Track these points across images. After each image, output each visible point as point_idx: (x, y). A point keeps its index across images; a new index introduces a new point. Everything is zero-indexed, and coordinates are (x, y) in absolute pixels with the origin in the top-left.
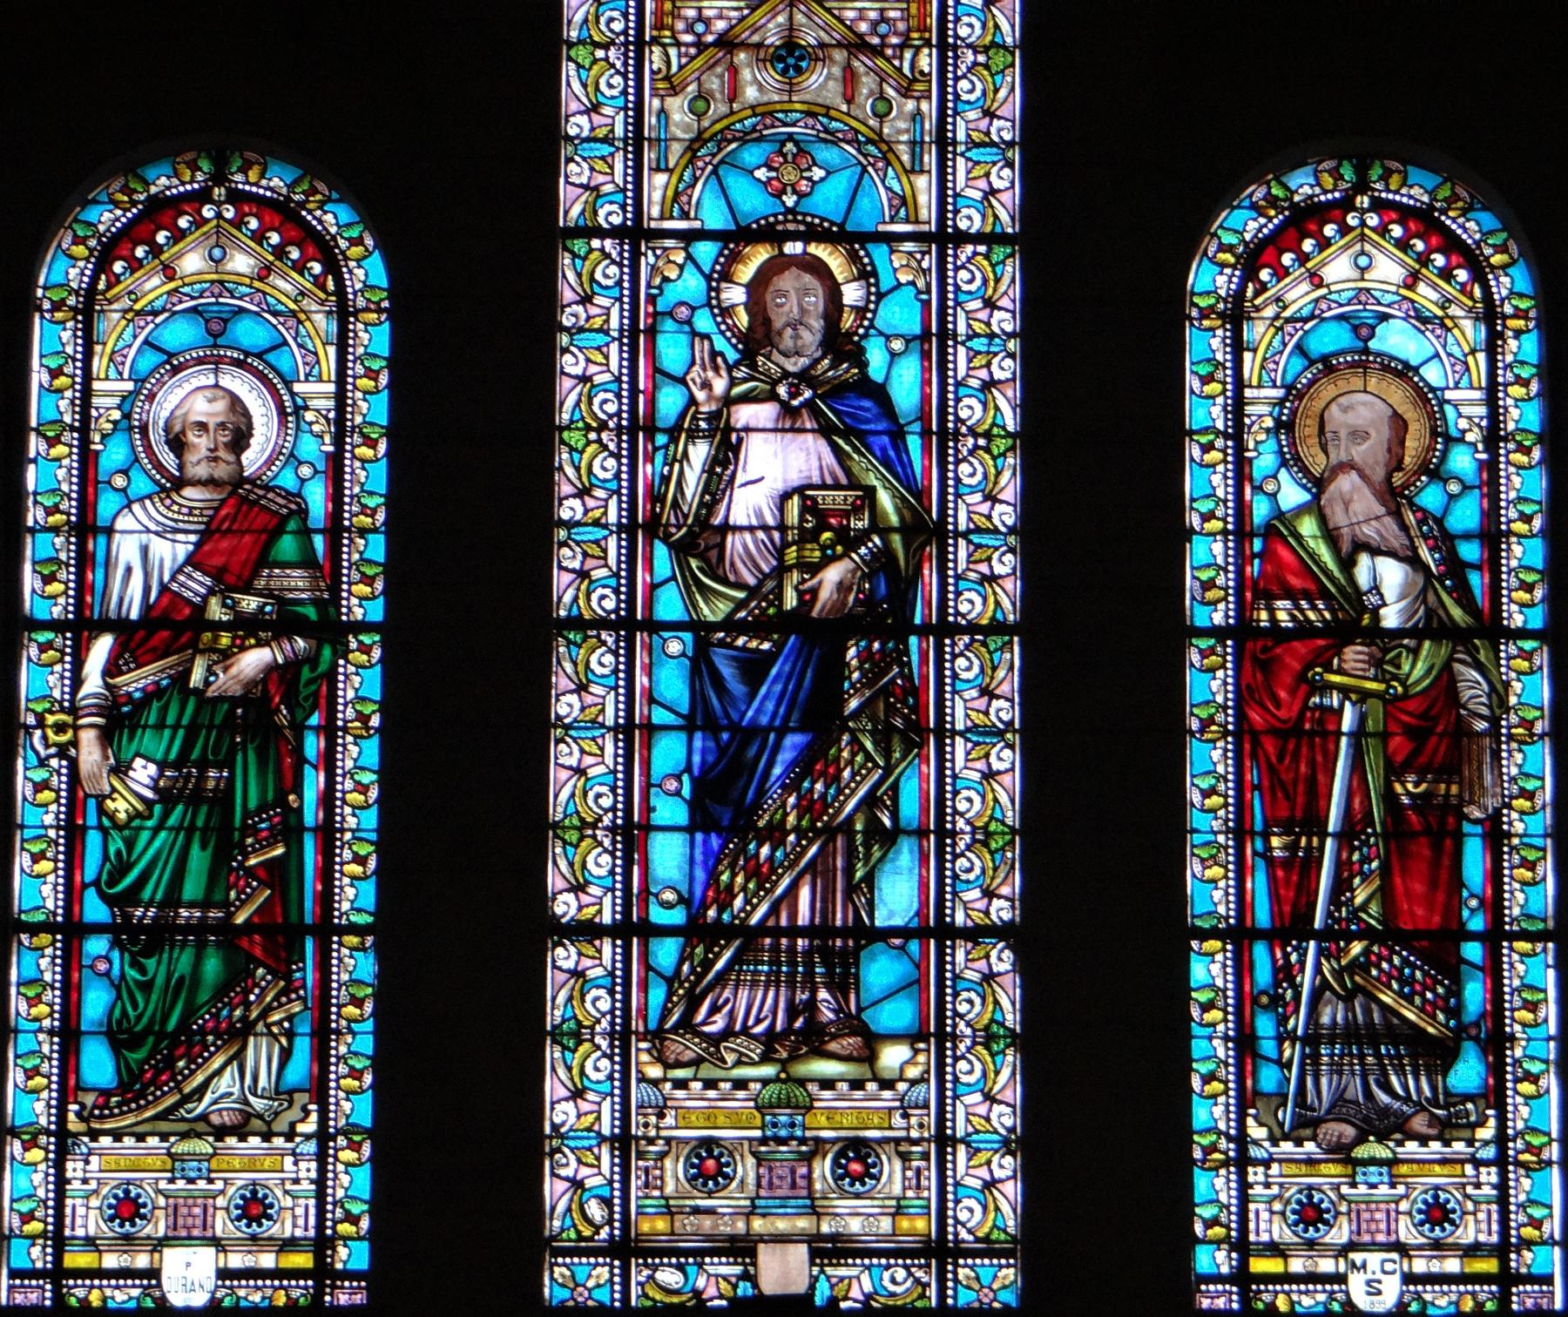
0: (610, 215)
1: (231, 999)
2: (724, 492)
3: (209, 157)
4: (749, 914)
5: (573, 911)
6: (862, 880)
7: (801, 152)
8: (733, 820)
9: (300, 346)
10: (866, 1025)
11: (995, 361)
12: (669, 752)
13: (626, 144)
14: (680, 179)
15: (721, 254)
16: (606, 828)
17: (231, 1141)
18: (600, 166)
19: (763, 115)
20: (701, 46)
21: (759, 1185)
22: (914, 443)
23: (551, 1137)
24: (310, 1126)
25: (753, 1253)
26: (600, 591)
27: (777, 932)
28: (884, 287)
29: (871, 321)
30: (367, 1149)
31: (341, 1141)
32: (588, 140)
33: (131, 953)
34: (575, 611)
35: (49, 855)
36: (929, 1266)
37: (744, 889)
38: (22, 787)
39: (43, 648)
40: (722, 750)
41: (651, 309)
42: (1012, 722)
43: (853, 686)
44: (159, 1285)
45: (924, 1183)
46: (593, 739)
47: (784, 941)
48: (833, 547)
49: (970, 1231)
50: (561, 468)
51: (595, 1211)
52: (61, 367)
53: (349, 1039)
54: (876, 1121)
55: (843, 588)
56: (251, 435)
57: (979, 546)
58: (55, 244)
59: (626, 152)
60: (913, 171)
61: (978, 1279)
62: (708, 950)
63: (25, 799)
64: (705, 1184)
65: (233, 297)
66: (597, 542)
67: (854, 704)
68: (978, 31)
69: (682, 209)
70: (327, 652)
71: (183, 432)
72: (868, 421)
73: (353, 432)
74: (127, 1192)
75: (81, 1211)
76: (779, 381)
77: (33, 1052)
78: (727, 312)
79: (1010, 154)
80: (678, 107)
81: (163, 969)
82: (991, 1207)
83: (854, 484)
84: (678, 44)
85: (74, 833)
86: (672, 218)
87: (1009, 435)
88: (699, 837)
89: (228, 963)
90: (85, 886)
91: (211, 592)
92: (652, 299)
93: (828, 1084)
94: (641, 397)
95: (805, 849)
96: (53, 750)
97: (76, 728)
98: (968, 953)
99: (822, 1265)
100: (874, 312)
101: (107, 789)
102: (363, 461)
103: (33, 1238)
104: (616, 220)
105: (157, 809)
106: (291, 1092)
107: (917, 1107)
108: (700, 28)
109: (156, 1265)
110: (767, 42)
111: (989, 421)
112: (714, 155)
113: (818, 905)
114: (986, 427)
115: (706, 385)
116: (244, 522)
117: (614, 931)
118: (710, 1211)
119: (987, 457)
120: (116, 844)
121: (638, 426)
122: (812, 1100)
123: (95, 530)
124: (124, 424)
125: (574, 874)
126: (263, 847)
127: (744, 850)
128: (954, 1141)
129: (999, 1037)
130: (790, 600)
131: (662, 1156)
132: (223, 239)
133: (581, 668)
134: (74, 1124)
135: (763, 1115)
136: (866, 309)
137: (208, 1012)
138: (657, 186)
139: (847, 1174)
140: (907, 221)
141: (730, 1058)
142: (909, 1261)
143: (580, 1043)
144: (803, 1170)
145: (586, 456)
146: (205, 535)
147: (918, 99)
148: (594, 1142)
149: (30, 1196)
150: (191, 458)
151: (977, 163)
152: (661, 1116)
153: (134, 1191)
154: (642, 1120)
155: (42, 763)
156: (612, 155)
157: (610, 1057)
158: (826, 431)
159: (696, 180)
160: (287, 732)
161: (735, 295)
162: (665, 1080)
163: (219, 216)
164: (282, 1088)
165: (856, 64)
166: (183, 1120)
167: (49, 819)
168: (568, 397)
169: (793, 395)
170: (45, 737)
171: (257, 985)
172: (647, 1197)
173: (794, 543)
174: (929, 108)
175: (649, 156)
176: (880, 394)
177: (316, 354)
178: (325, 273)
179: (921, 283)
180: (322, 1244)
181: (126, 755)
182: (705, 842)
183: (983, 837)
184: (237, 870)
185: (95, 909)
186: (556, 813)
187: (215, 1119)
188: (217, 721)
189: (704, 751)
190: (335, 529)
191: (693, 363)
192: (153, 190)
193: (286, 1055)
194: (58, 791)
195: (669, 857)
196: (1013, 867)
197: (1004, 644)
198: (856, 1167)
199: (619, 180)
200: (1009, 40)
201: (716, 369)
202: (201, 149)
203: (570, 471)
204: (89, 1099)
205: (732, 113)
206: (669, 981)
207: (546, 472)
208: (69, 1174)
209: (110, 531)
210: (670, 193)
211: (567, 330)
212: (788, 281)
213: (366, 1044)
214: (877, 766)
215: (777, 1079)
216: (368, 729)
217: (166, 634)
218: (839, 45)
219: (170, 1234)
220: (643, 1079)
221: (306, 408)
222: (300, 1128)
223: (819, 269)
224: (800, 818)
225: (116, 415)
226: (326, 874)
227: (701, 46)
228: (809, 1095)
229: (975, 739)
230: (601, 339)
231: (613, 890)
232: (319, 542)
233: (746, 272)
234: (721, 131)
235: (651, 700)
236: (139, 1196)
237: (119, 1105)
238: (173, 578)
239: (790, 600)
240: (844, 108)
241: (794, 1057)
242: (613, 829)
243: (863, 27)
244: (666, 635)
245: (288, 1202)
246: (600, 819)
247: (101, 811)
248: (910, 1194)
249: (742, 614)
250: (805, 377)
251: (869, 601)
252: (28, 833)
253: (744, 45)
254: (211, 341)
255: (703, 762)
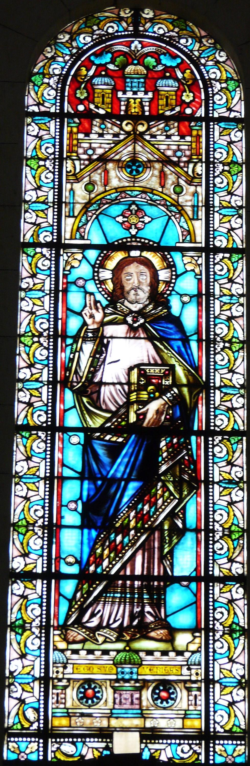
0: (45, 237)
2: (100, 366)
4: (111, 569)
5: (22, 566)
6: (168, 553)
7: (139, 209)
8: (103, 523)
10: (169, 624)
11: (234, 308)
12: (71, 490)
13: (54, 205)
14: (80, 221)
15: (99, 256)
16: (40, 526)
18: (41, 214)
19: (121, 192)
20: (91, 161)
21: (114, 703)
22: (194, 345)
23: (9, 678)
25: (111, 737)
26: (38, 413)
27: (125, 578)
28: (179, 273)
29: (173, 287)
32: (35, 202)
34: (25, 422)
36: (200, 744)
37: (109, 557)
40: (98, 489)
41: (65, 281)
42: (241, 479)
43: (163, 459)
45: (198, 702)
46: (34, 483)
47: (128, 582)
48: (154, 393)
49: (222, 727)
50: (20, 354)
51: (31, 714)
54: (175, 671)
55: (158, 412)
57: (226, 394)
59: (54, 208)
60: (193, 219)
61: (225, 751)
62: (90, 586)
64: (87, 702)
66: (37, 389)
67: (164, 468)
68: (225, 155)
69: (81, 235)
72: (171, 334)
76: (128, 315)
78: (102, 282)
79: (240, 212)
80: (79, 188)
82: (233, 715)
83: (164, 363)
84: (80, 159)
86: (76, 239)
87: (241, 342)
88: (86, 531)
92: (65, 276)
93: (150, 653)
94: (60, 322)
95: (139, 538)
98: (221, 589)
99: (146, 743)
100: (174, 283)
104: (49, 239)
107: (195, 665)
108: (90, 152)
110: (123, 159)
111: (231, 335)
112: (97, 210)
113: (146, 565)
114: (230, 338)
115: (92, 316)
117: (42, 576)
118: (90, 715)
119: (230, 352)
121: (58, 335)
122: (142, 661)
125: (23, 548)
127: (108, 538)
128: (214, 682)
129: (237, 631)
130: (133, 418)
131: (65, 687)
133: (28, 449)
135: (117, 668)
136: (170, 282)
138: (68, 224)
139: (159, 697)
140: (191, 242)
141: (101, 639)
142: (190, 742)
143: (24, 630)
144: (137, 695)
145: (32, 349)
147: (196, 186)
148: (31, 680)
151: (225, 216)
152: (65, 667)
154: (55, 669)
156: (47, 209)
157: (40, 638)
158: (150, 338)
159: (88, 221)
161: (106, 275)
162: (67, 649)
165: (166, 169)
168: (23, 319)
169: (134, 322)
172: (57, 708)
173: (135, 391)
174: (201, 190)
175: (65, 210)
176: (177, 322)
179: (197, 271)
182: (89, 534)
183: (228, 533)
186: (14, 519)
189: (89, 490)
191: (85, 306)
195: (72, 542)
196: (243, 548)
197: (239, 441)
198: (164, 694)
199: (50, 220)
200: (240, 160)
201: (97, 309)
203: (24, 356)
205: (106, 191)
206: (70, 601)
207: (13, 355)
210: (75, 228)
211: (24, 290)
212: (133, 268)
214: (175, 498)
215: (124, 650)
218: (158, 161)
220: (56, 649)
223: (148, 263)
224: (137, 523)
227: (91, 161)
228: (141, 658)
229: (224, 485)
230: (40, 294)
231: (42, 556)
233: (111, 264)
234: (100, 199)
235: (63, 465)
239: (133, 418)
240: (160, 190)
241: (133, 639)
242: (43, 527)
243: (169, 153)
244: (70, 434)
246: (36, 522)
248: (191, 708)
249: (109, 424)
250: (141, 313)
251: (172, 419)
253: (112, 160)
255: (88, 495)
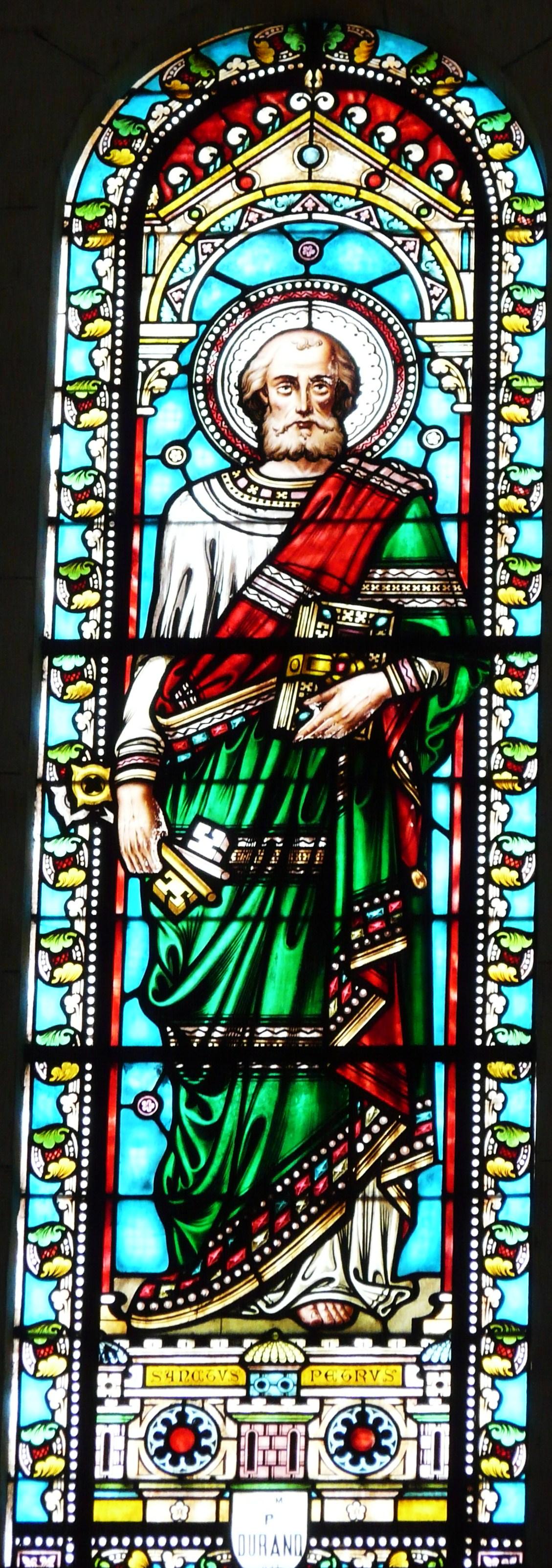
1: (331, 1151)
3: (299, 31)
9: (424, 275)
17: (330, 1345)
24: (443, 1323)
30: (522, 1354)
31: (487, 1344)
33: (189, 1088)
35: (77, 954)
38: (39, 865)
39: (69, 677)
44: (227, 1545)
52: (95, 307)
53: (497, 1203)
56: (356, 393)
58: (88, 147)
63: (42, 879)
65: (332, 212)
70: (463, 679)
71: (264, 389)
73: (498, 386)
74: (182, 1416)
75: (117, 1443)
77: (52, 1224)
81: (234, 1108)
85: (109, 927)
89: (324, 1099)
90: (125, 997)
91: (303, 600)
96: (82, 814)
97: (115, 785)
101: (157, 867)
102: (512, 424)
103: (50, 1480)
105: (227, 892)
106: (415, 1277)
109: (224, 1518)
116: (347, 507)
120: (169, 939)
123: (142, 521)
124: (182, 380)
126: (374, 943)
132: (318, 137)
134: (109, 1323)
137: (298, 1167)
146: (294, 527)
149: (44, 1423)
150: (273, 423)
153: (192, 1414)
155: (66, 831)
160: (409, 787)
163: (312, 106)
164: (401, 1272)
166: (262, 1316)
167: (76, 907)
170: (71, 797)
171: (368, 1130)
177: (446, 284)
178: (458, 177)
180: (461, 1487)
181: (184, 819)
184: (339, 973)
185: (138, 1029)
187: (308, 1315)
188: (311, 772)
190: (475, 515)
192: (223, 75)
193: (408, 1225)
194: (89, 870)
202: (291, 22)
204: (130, 1288)
208: (101, 1392)
209: (161, 522)
213: (519, 1210)
216: (521, 782)
217: (238, 658)
219: (244, 1474)
221: (434, 356)
222: (429, 1327)
225: (171, 368)
226: (465, 977)
232: (451, 531)
236: (199, 1421)
237: (172, 1296)
238: (249, 582)
245: (409, 1429)
247: (148, 895)
252: (46, 927)
254: (301, 269)
